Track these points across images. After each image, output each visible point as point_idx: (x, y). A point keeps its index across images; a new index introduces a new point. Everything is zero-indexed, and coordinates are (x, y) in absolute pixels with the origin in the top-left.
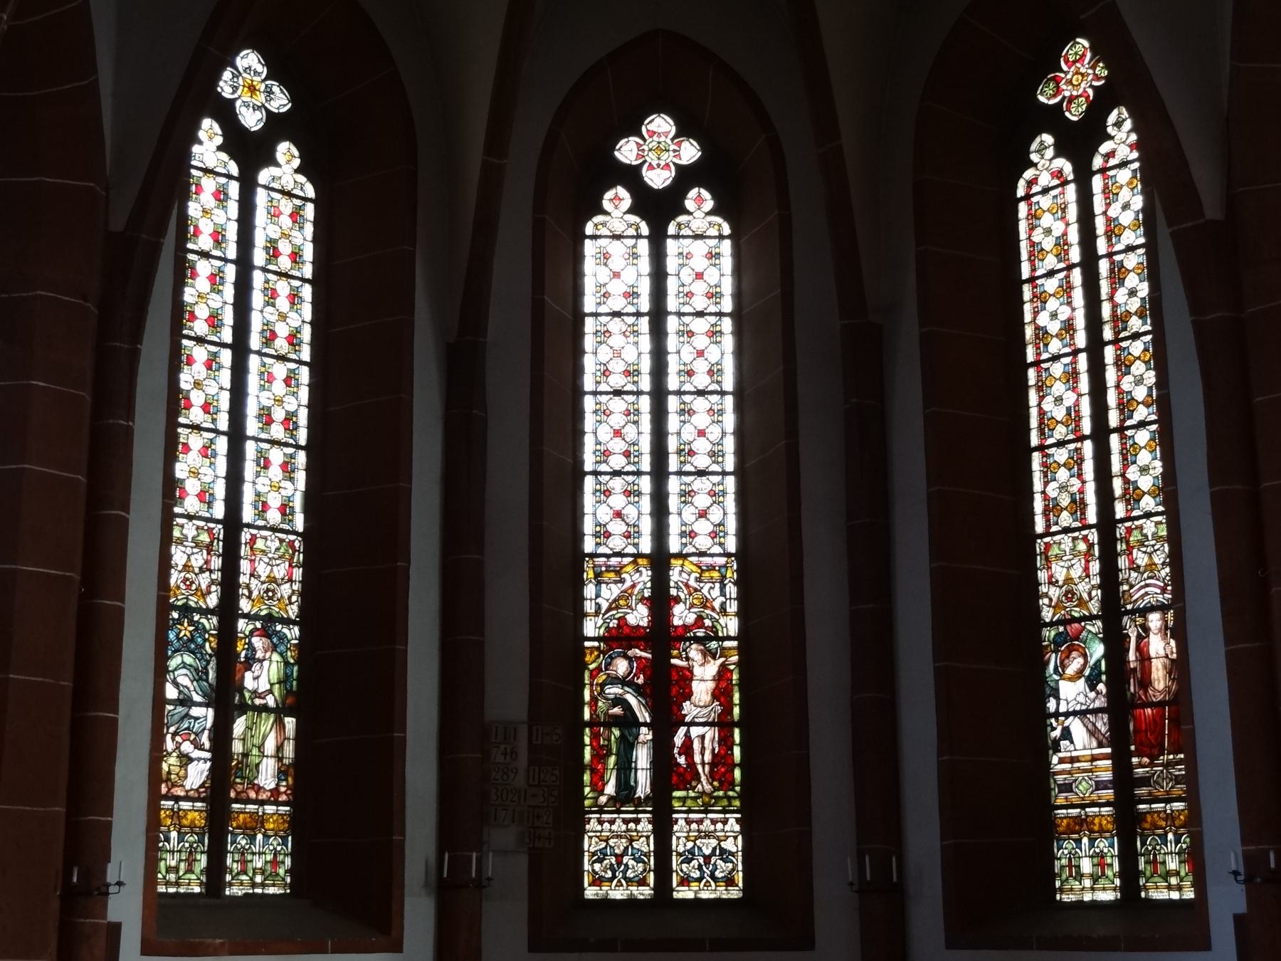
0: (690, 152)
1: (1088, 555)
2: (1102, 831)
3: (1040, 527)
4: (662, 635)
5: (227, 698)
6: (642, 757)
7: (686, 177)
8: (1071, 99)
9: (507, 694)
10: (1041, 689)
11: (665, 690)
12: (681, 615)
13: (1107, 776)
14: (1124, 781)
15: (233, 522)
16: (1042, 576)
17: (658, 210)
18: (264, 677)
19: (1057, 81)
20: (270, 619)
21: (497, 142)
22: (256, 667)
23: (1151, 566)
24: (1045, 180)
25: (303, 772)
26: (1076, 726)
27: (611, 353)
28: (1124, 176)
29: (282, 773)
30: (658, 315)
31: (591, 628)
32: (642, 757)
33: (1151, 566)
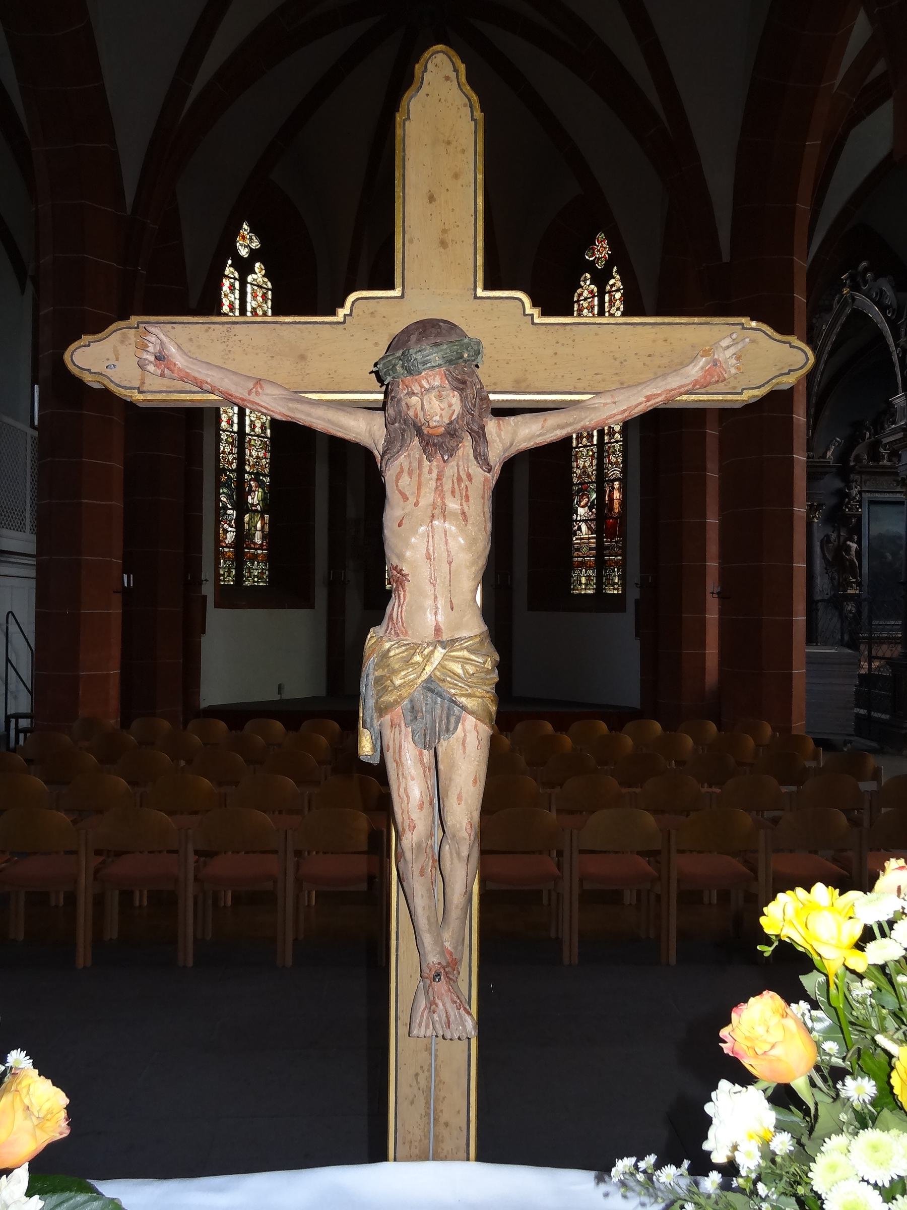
1: (593, 456)
2: (590, 567)
3: (574, 445)
5: (242, 507)
8: (599, 259)
13: (594, 545)
16: (574, 464)
18: (255, 498)
19: (593, 249)
20: (258, 474)
22: (253, 494)
23: (617, 463)
24: (586, 294)
26: (584, 527)
28: (618, 295)
29: (264, 538)
33: (617, 463)
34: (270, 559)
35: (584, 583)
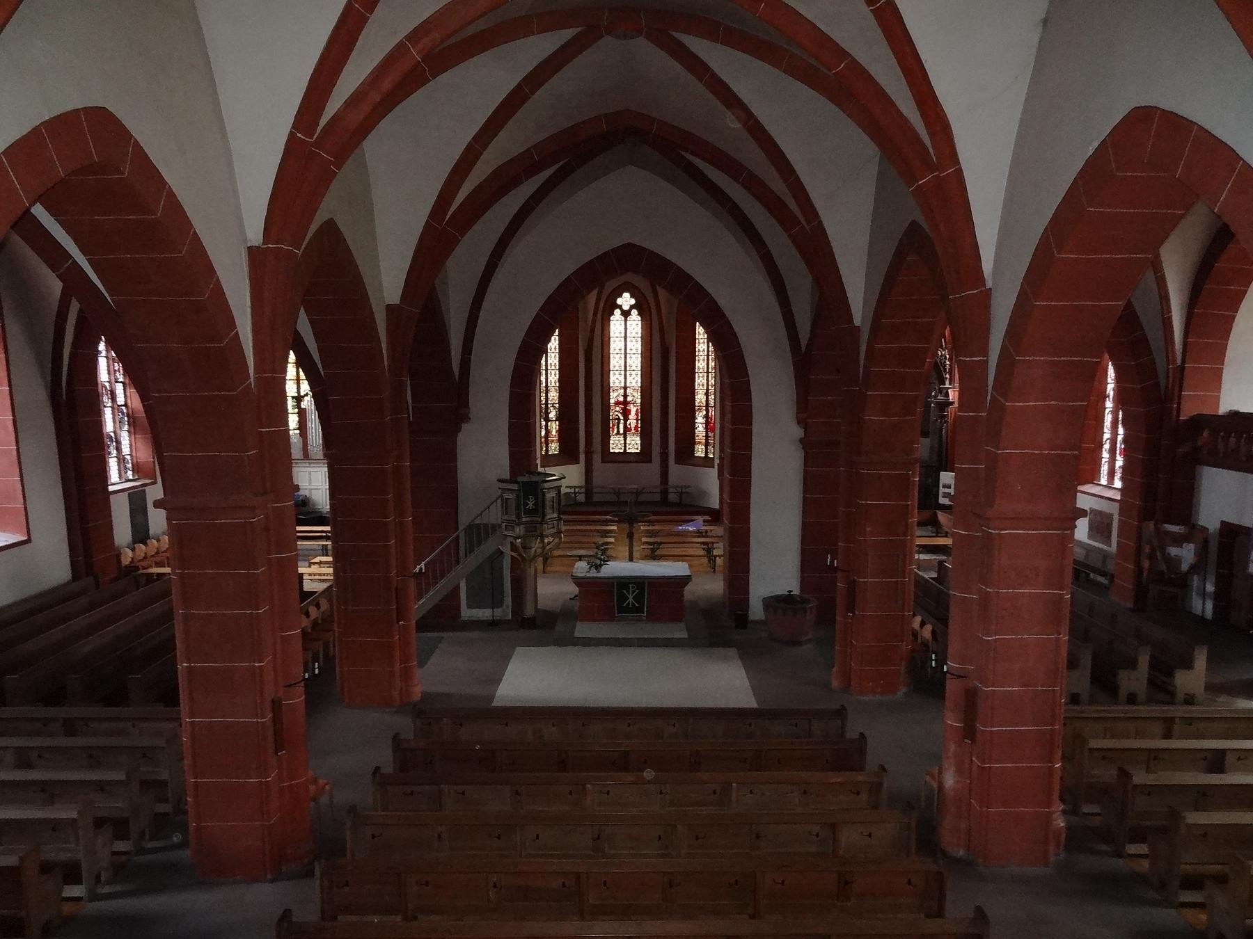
0: (633, 301)
4: (625, 403)
5: (547, 420)
6: (621, 426)
7: (632, 307)
9: (597, 418)
10: (694, 418)
11: (626, 413)
12: (629, 399)
14: (707, 436)
15: (547, 386)
17: (626, 314)
18: (552, 415)
21: (595, 314)
25: (559, 431)
27: (616, 345)
30: (625, 338)
31: (612, 401)
32: (621, 426)
34: (559, 441)
35: (700, 451)
